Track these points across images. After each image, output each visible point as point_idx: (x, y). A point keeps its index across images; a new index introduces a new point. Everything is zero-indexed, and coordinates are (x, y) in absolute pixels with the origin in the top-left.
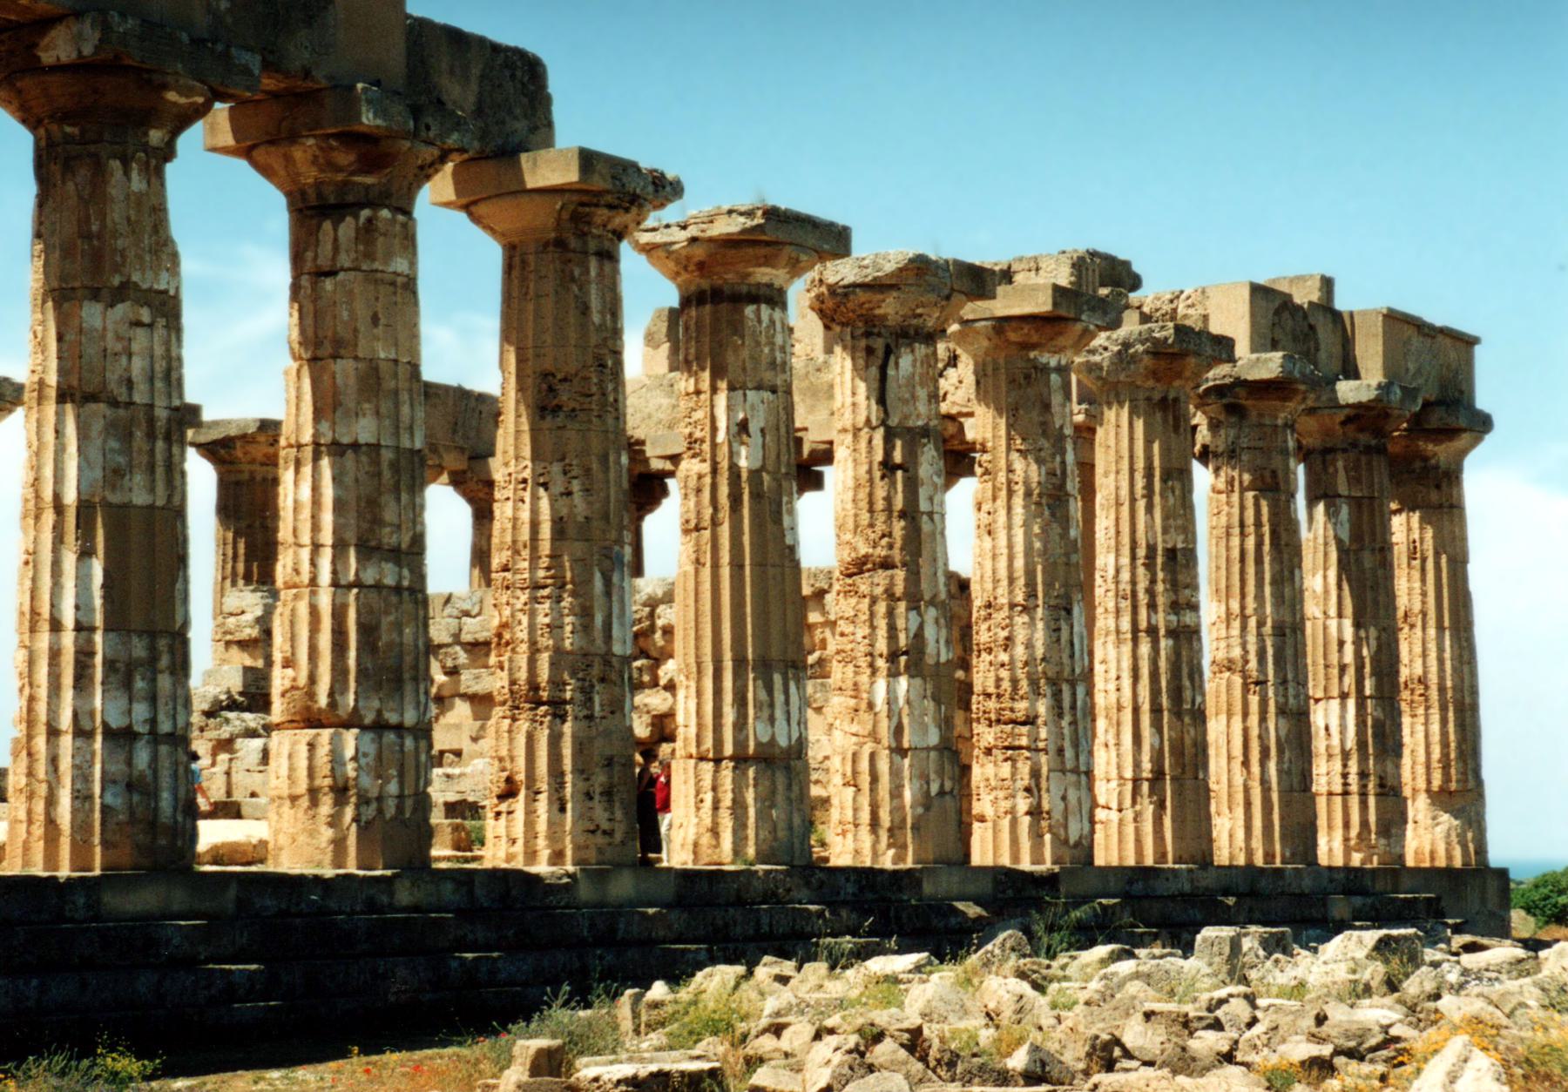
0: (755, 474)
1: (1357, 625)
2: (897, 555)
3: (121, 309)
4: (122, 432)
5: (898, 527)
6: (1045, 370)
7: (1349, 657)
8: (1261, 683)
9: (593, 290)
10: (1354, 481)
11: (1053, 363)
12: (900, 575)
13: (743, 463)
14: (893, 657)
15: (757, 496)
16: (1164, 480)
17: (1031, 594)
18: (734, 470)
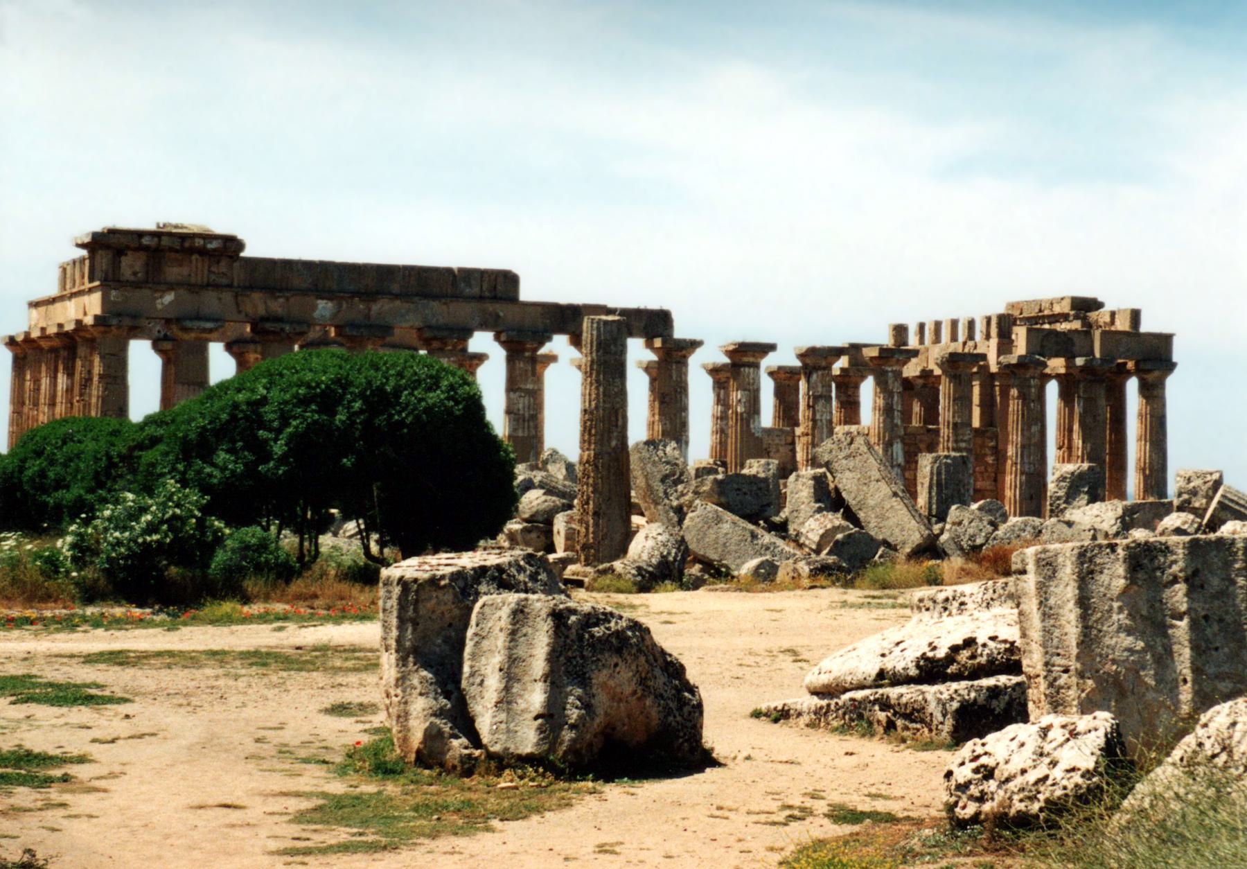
0: (742, 414)
1: (1083, 442)
2: (810, 432)
3: (517, 394)
4: (517, 420)
5: (810, 424)
6: (887, 372)
7: (1080, 454)
8: (1016, 464)
9: (674, 372)
10: (1085, 392)
11: (890, 369)
12: (810, 437)
13: (739, 410)
14: (807, 461)
15: (742, 419)
16: (954, 400)
17: (879, 440)
18: (737, 412)
